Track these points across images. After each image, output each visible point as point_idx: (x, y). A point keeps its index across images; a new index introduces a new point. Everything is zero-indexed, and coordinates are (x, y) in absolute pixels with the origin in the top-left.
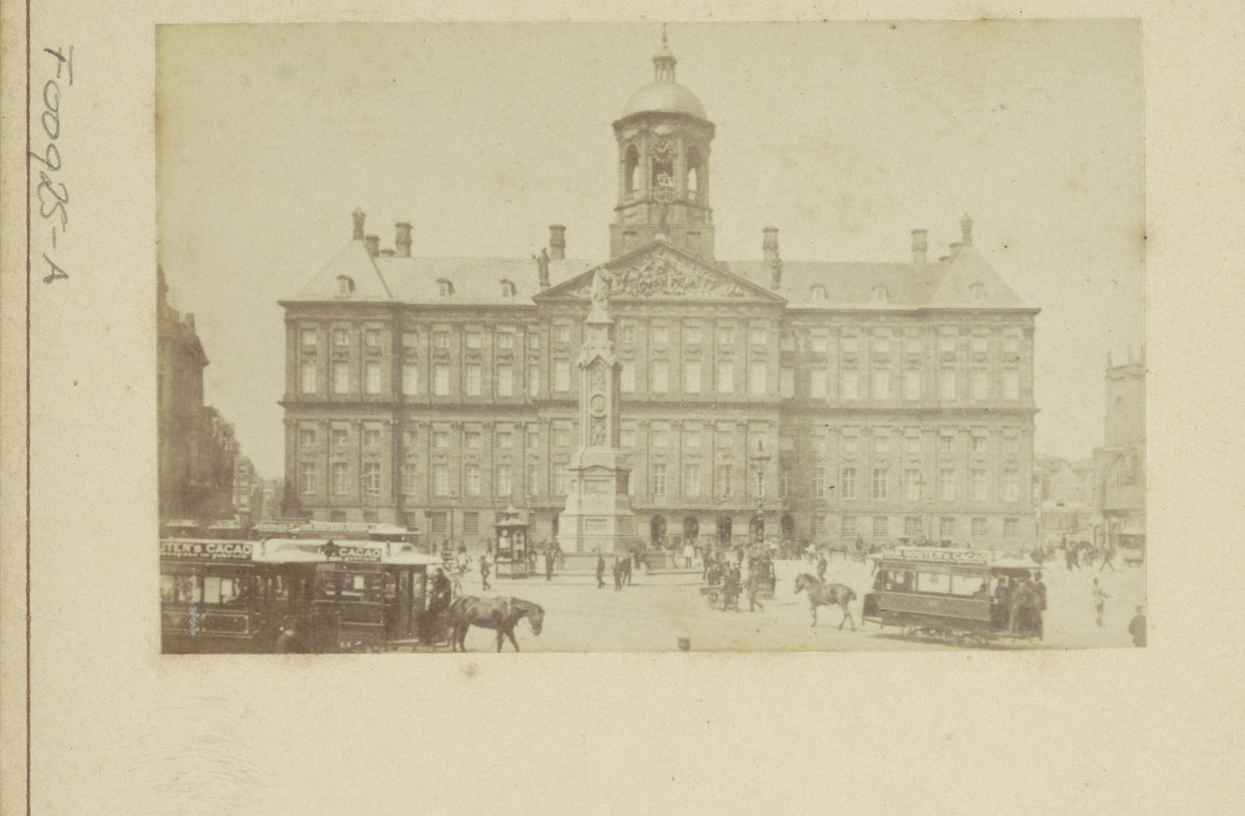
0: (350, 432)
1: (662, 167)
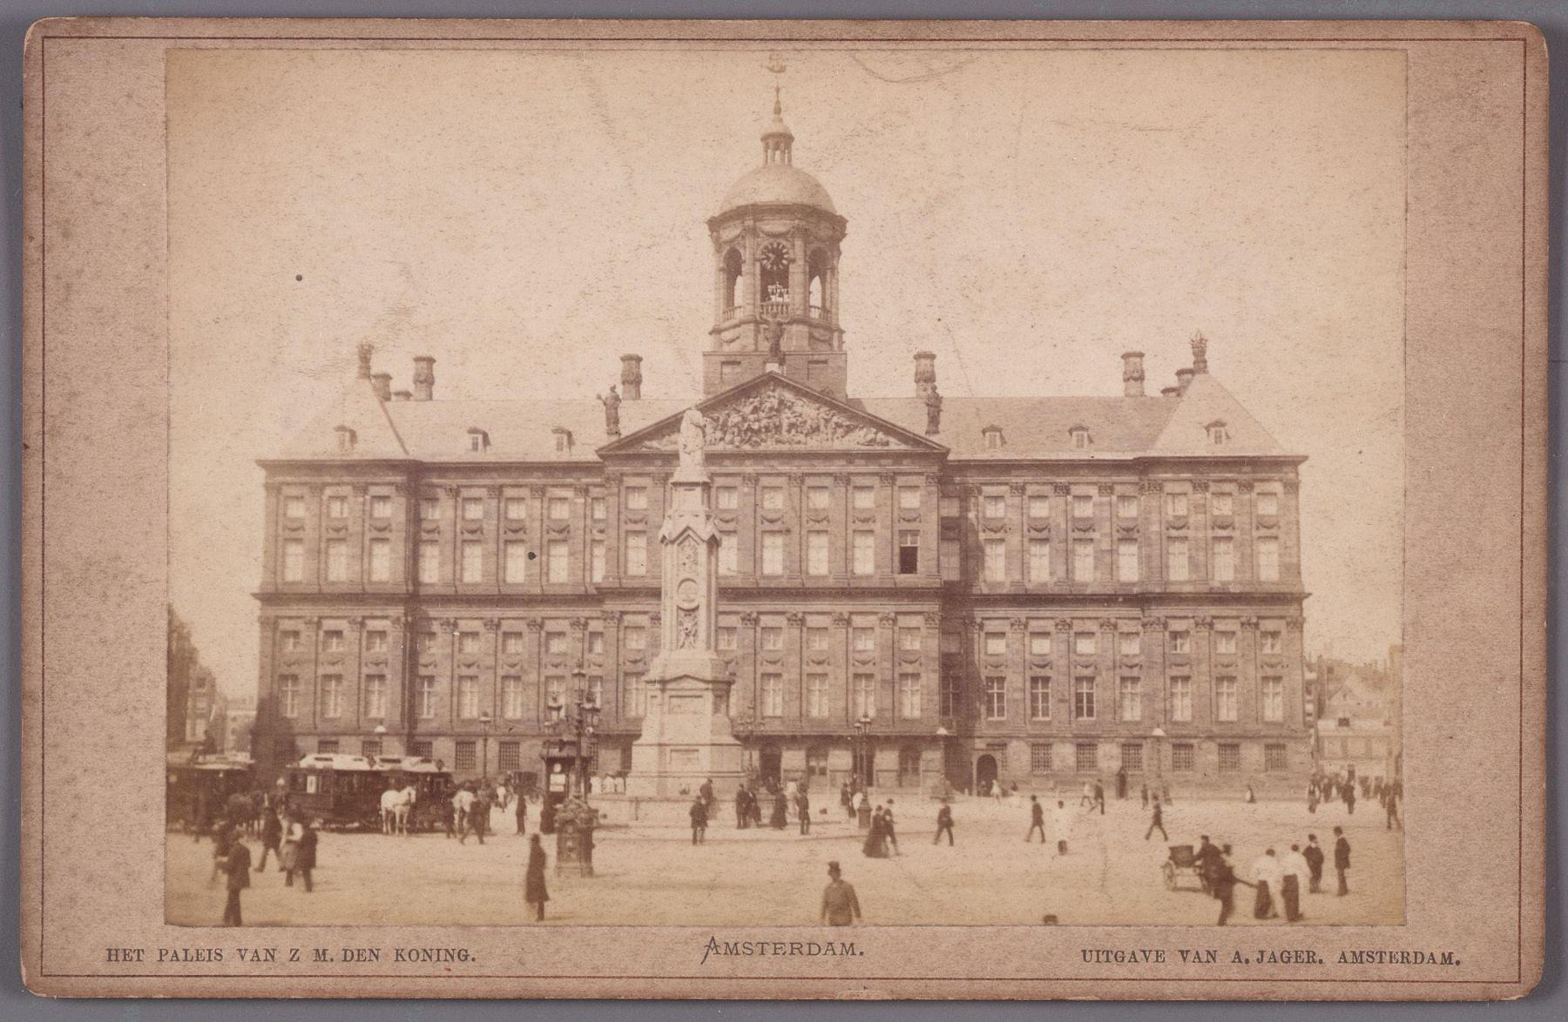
0: (346, 633)
1: (775, 275)
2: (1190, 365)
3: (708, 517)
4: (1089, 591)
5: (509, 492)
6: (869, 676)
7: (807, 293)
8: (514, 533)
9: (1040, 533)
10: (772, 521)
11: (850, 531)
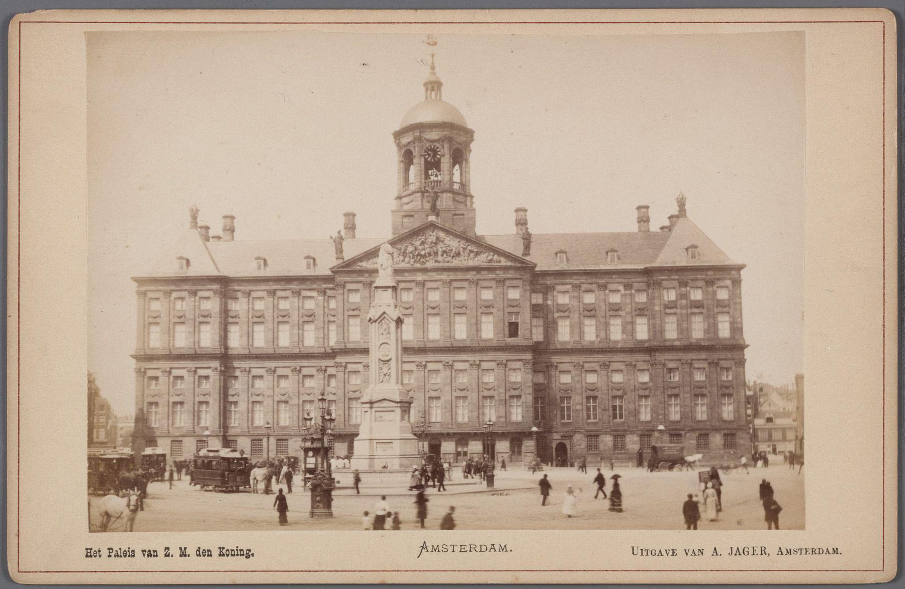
0: (186, 377)
1: (432, 165)
2: (676, 213)
3: (396, 306)
4: (620, 346)
5: (280, 294)
6: (491, 397)
7: (452, 174)
8: (283, 318)
9: (590, 312)
10: (433, 308)
11: (479, 313)
